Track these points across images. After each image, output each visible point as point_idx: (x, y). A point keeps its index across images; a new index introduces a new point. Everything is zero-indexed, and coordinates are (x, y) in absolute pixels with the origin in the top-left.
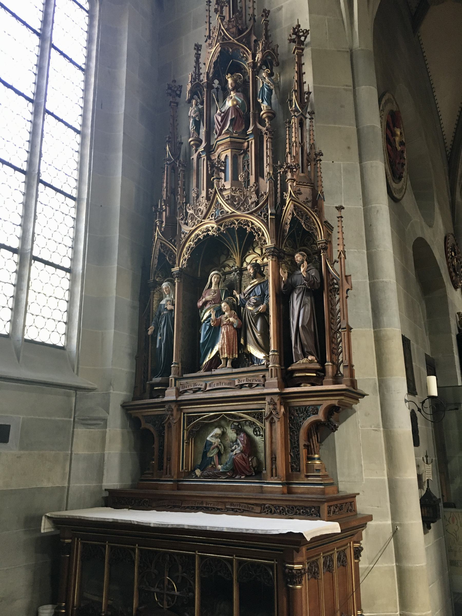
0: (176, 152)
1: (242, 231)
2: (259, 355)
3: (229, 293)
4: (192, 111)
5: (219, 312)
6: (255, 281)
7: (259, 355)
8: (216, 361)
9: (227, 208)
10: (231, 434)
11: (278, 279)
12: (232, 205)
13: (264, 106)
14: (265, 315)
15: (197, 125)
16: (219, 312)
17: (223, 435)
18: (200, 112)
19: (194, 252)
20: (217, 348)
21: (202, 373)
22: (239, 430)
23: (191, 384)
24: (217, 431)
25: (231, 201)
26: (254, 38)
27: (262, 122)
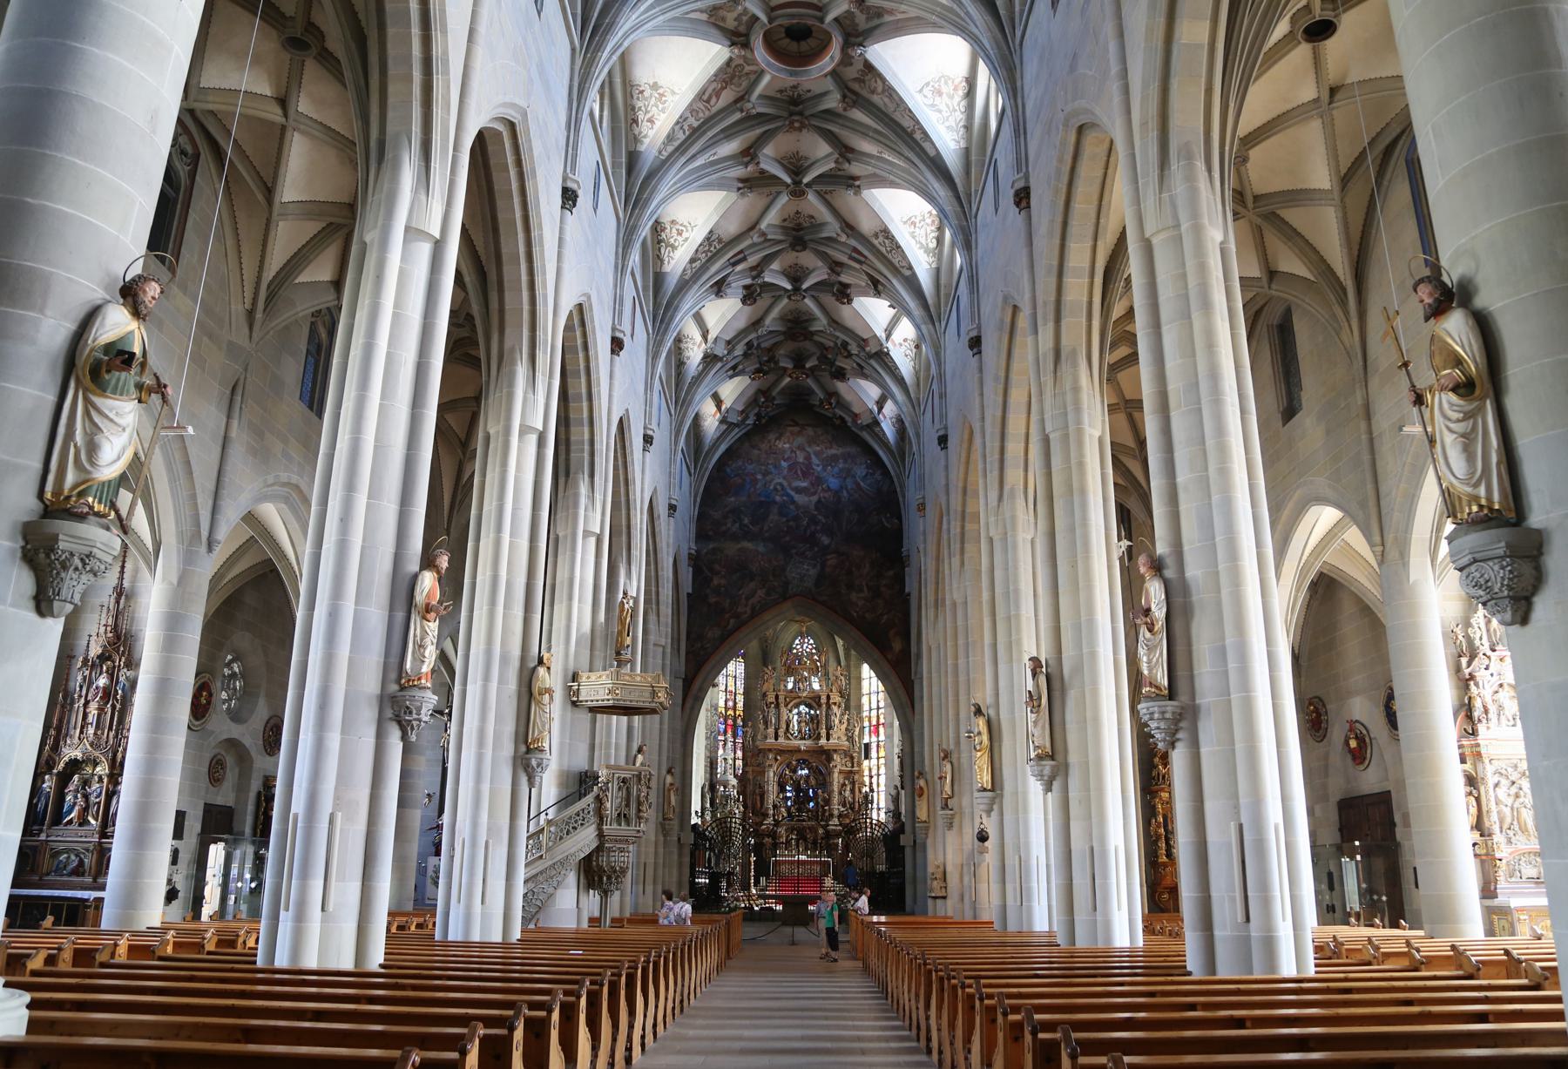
0: (65, 698)
1: (95, 760)
2: (93, 822)
3: (84, 788)
4: (80, 678)
5: (76, 797)
6: (98, 785)
7: (93, 822)
8: (70, 822)
9: (89, 747)
10: (73, 857)
11: (107, 789)
12: (91, 746)
13: (120, 692)
14: (99, 803)
15: (81, 687)
16: (76, 797)
17: (69, 857)
18: (85, 678)
19: (67, 764)
20: (72, 815)
21: (61, 827)
22: (77, 856)
23: (55, 833)
24: (65, 855)
25: (92, 745)
26: (122, 649)
27: (117, 701)
